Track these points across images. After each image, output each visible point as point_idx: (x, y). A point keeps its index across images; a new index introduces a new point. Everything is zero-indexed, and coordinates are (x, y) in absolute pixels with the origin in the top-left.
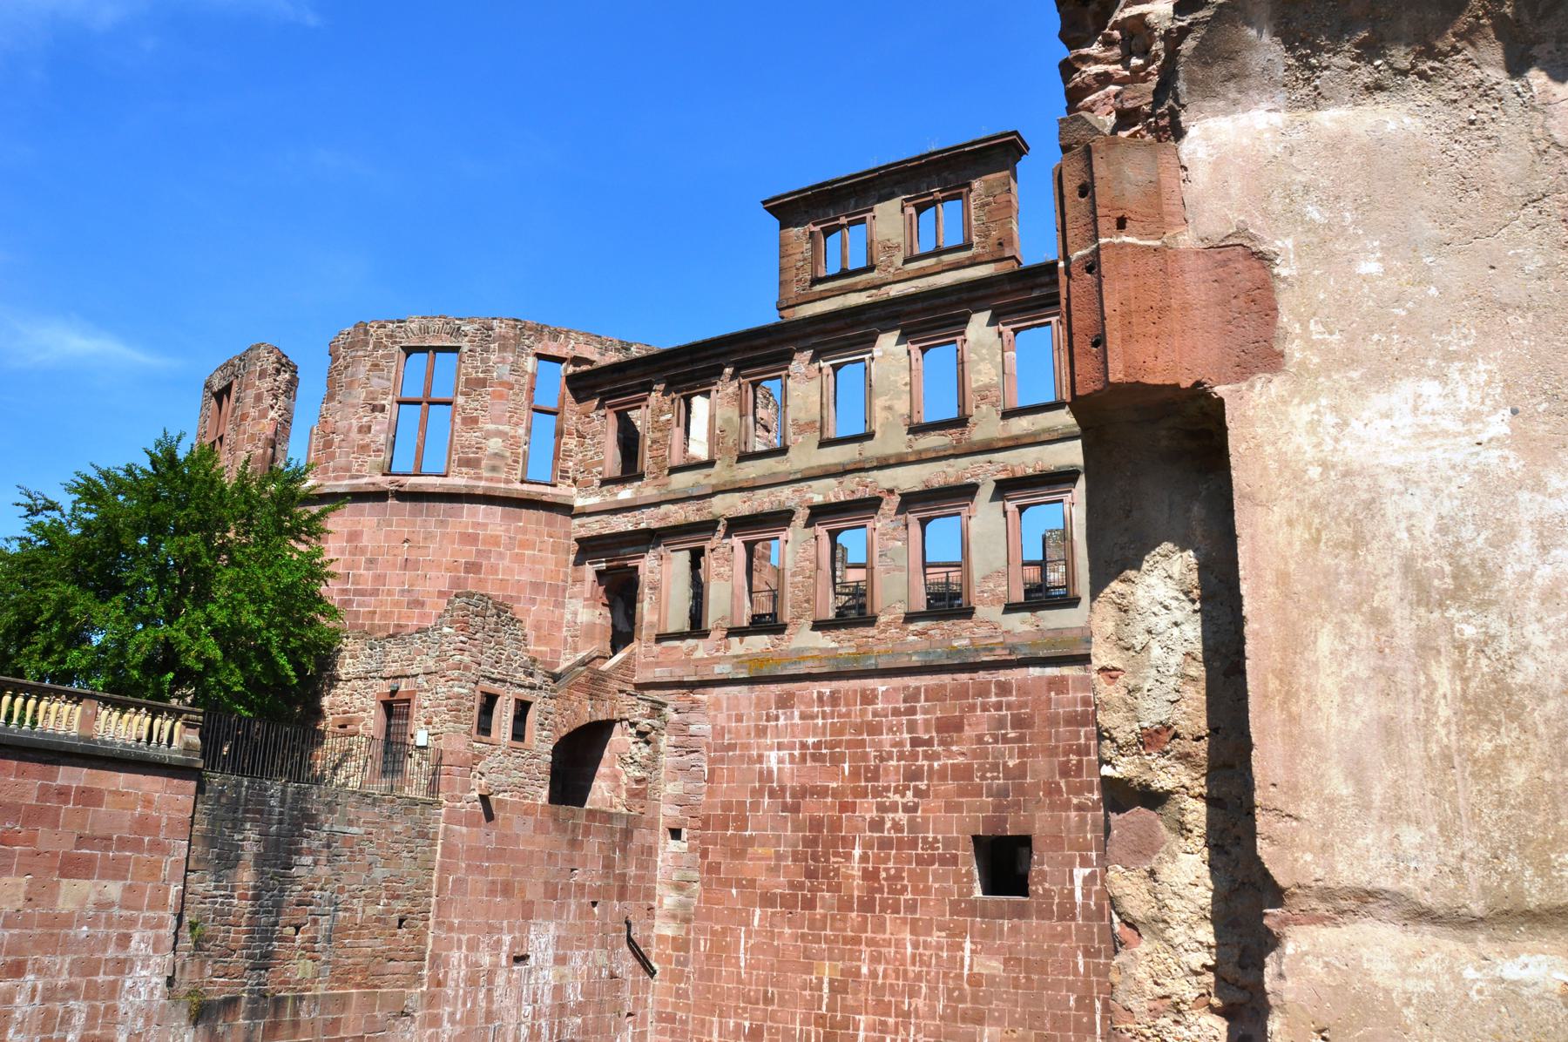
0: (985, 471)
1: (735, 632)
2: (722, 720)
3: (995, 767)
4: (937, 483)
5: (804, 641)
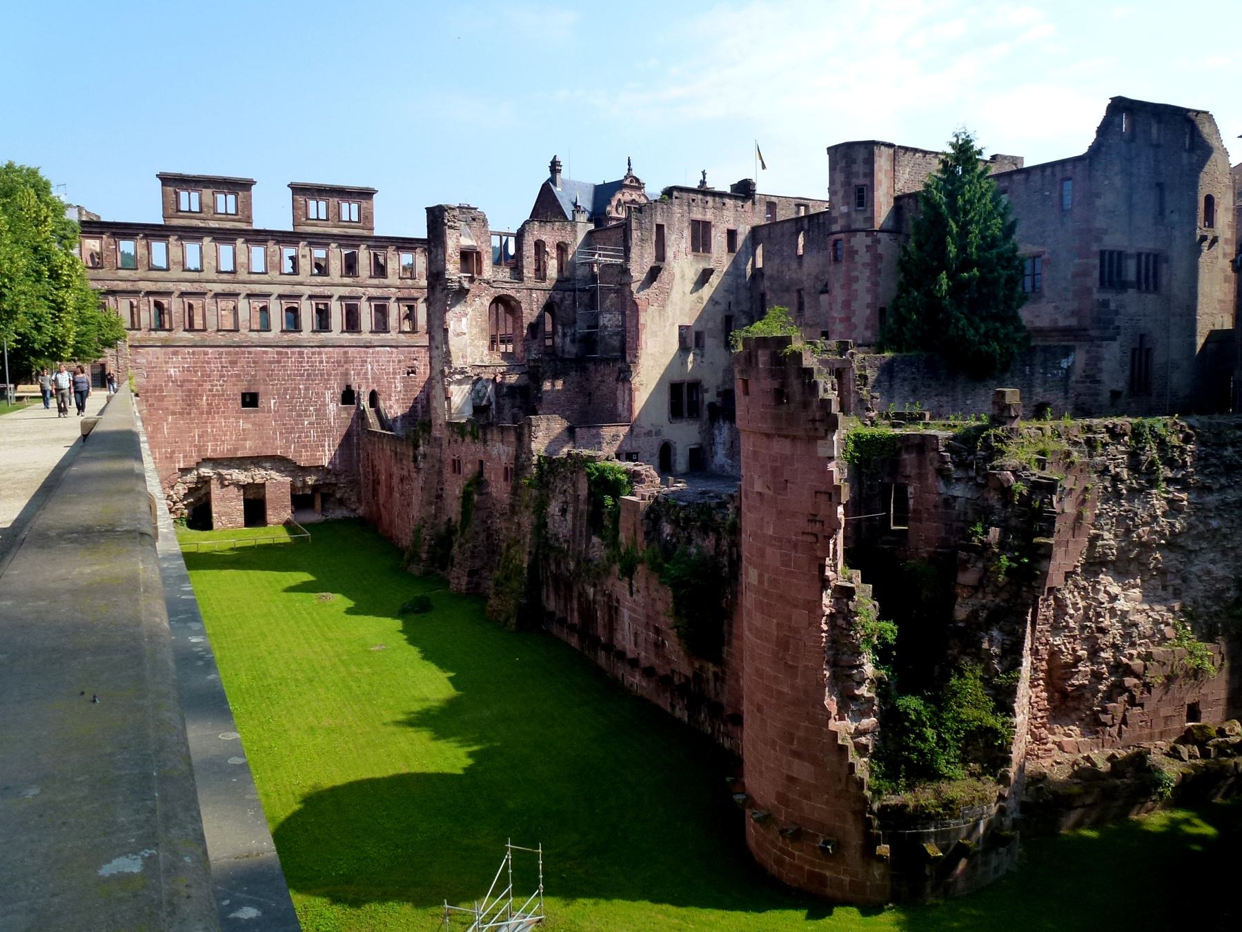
0: (244, 289)
1: (151, 330)
2: (150, 358)
4: (227, 290)
5: (181, 335)
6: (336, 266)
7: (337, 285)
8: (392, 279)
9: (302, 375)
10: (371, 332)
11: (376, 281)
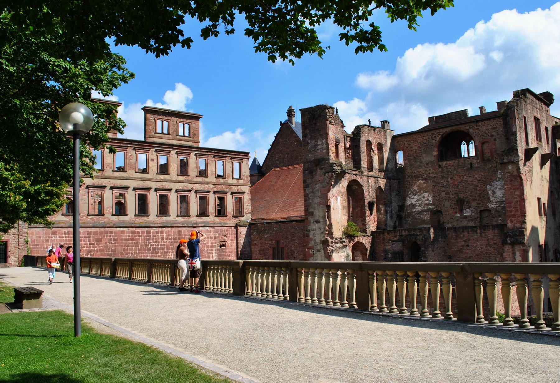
2: (34, 237)
3: (109, 249)
4: (96, 184)
6: (174, 168)
7: (174, 182)
8: (211, 178)
9: (149, 249)
10: (197, 216)
11: (200, 179)
